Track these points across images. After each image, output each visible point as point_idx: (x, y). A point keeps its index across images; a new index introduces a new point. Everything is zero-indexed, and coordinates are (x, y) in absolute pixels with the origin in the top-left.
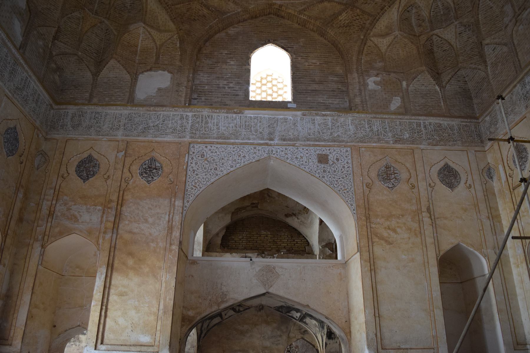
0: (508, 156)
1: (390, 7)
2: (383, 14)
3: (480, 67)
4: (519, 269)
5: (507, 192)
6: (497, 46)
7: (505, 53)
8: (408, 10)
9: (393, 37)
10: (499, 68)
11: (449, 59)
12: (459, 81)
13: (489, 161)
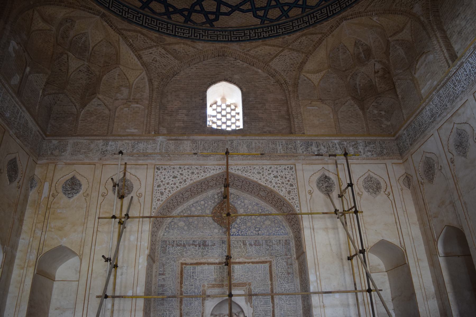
0: (59, 180)
1: (65, 6)
2: (57, 5)
3: (77, 104)
4: (22, 271)
5: (43, 206)
6: (104, 105)
7: (105, 114)
8: (68, 20)
9: (49, 28)
10: (92, 118)
11: (60, 78)
12: (54, 99)
13: (36, 173)
